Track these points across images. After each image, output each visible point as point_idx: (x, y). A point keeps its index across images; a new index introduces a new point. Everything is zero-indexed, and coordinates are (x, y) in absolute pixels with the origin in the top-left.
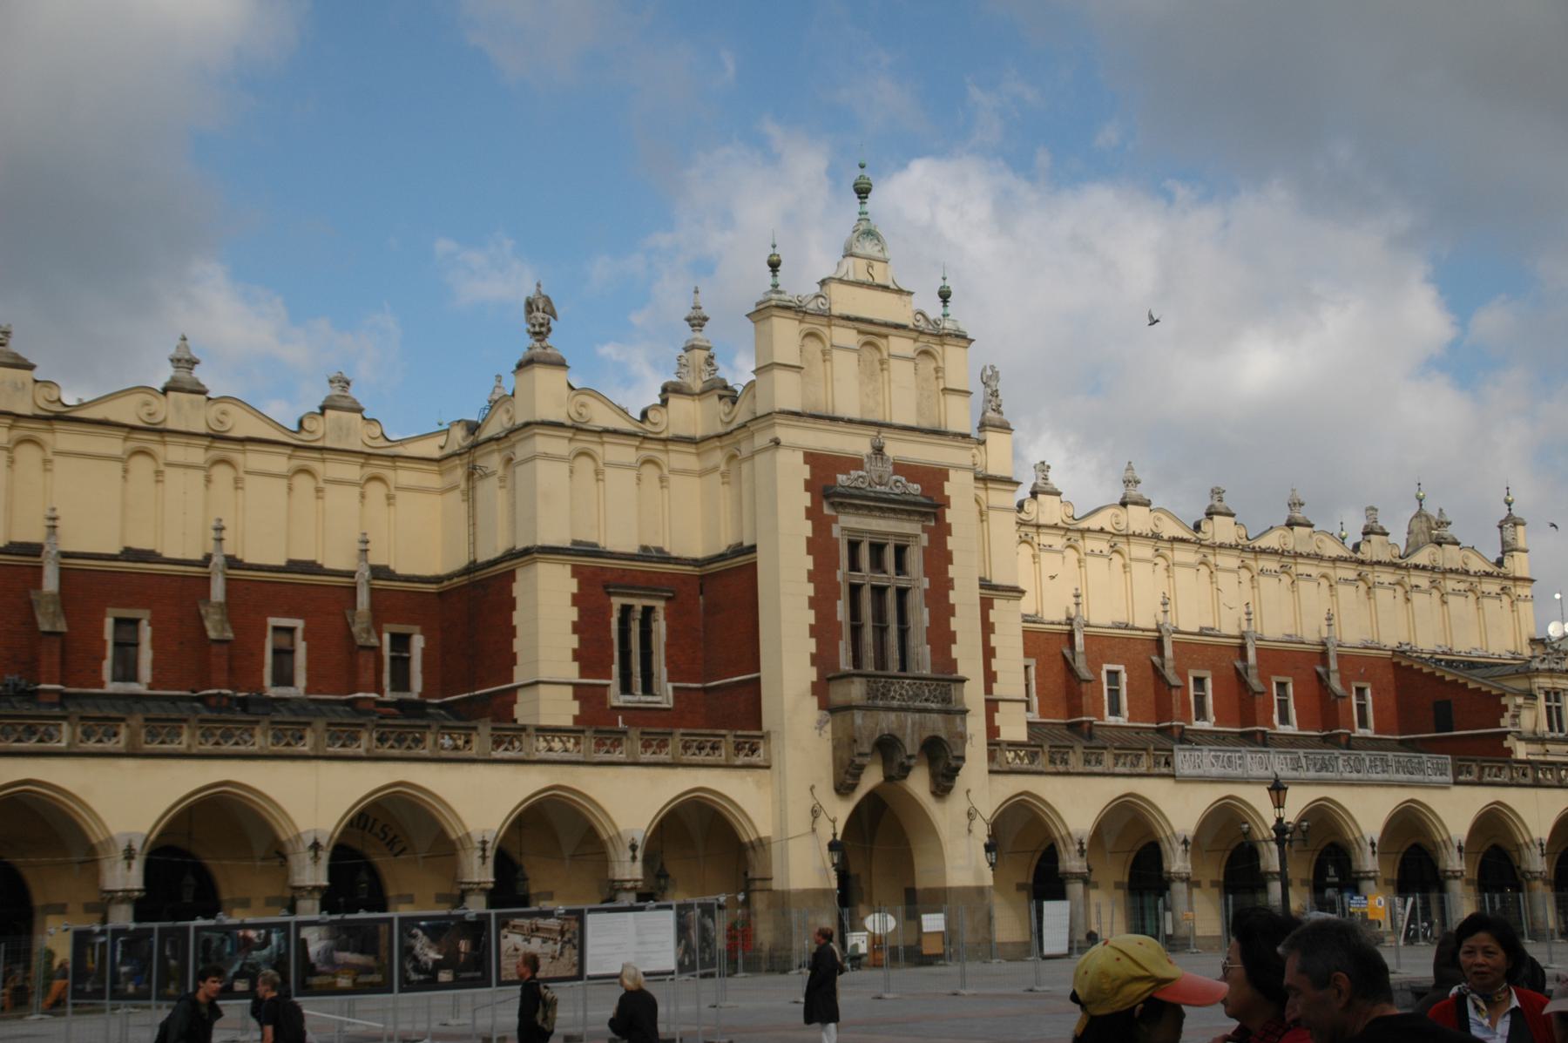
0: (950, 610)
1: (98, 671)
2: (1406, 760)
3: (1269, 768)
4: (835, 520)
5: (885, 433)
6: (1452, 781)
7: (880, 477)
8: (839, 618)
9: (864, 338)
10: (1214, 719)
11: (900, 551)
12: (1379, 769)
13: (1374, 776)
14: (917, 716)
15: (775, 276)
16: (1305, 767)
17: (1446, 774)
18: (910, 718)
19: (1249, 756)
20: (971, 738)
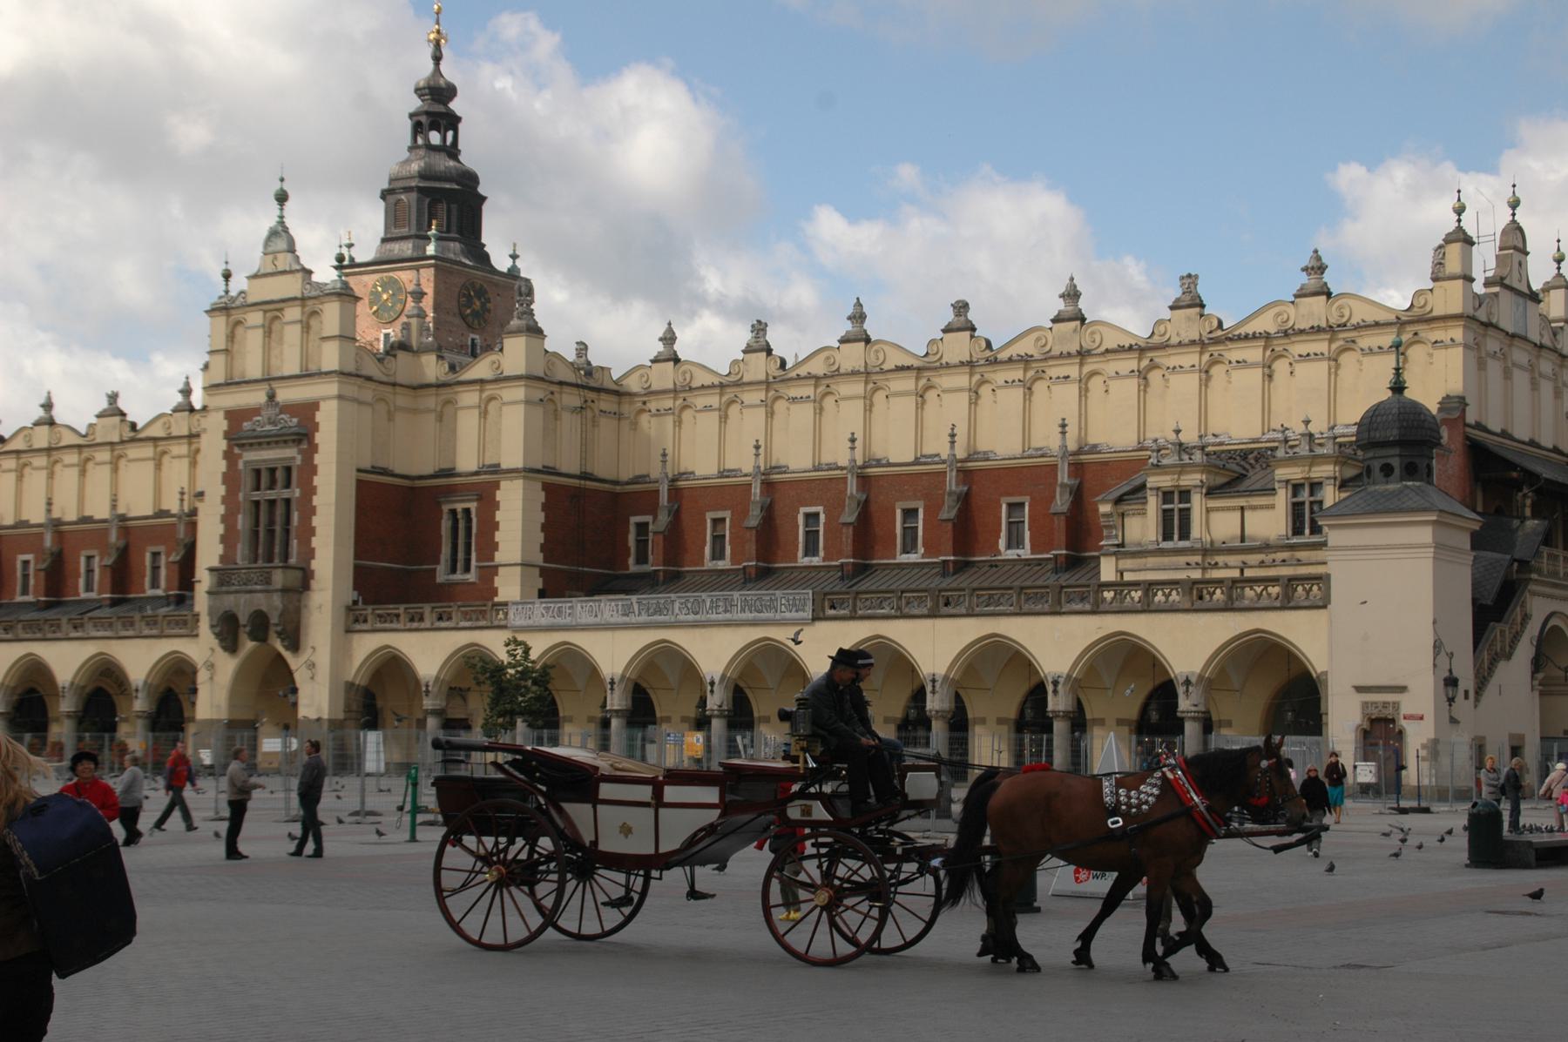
0: (313, 511)
1: (143, 584)
2: (755, 598)
3: (599, 616)
4: (240, 456)
5: (275, 385)
6: (810, 617)
7: (269, 419)
8: (239, 526)
9: (269, 315)
10: (921, 550)
11: (288, 470)
12: (721, 610)
13: (714, 616)
14: (248, 596)
15: (227, 285)
16: (637, 613)
17: (804, 610)
18: (243, 598)
19: (579, 605)
20: (320, 607)
